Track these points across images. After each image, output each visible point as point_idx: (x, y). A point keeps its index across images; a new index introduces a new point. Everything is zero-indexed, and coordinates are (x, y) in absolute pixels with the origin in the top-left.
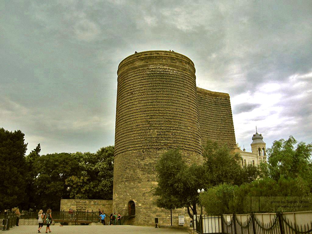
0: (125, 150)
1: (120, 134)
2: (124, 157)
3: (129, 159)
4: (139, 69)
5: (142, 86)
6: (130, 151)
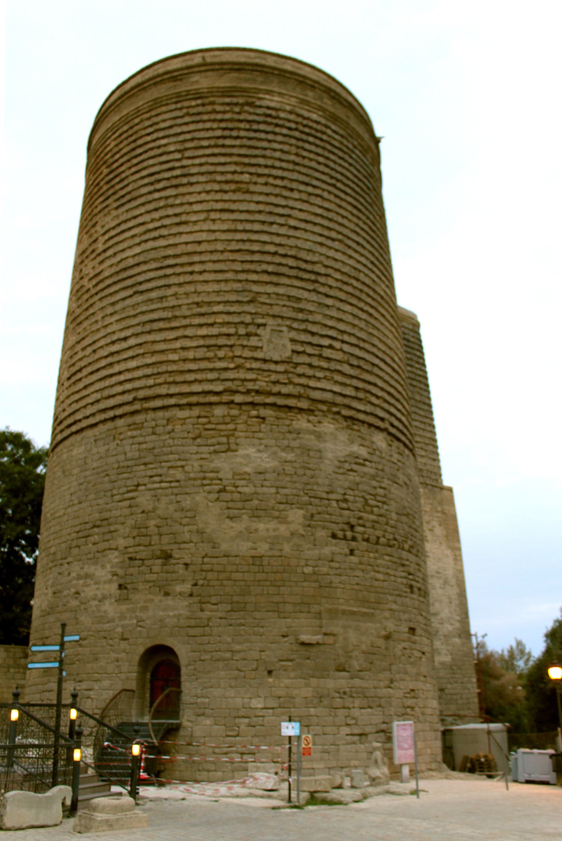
0: (127, 409)
1: (102, 342)
2: (122, 437)
3: (150, 445)
4: (212, 99)
5: (222, 160)
6: (160, 414)
